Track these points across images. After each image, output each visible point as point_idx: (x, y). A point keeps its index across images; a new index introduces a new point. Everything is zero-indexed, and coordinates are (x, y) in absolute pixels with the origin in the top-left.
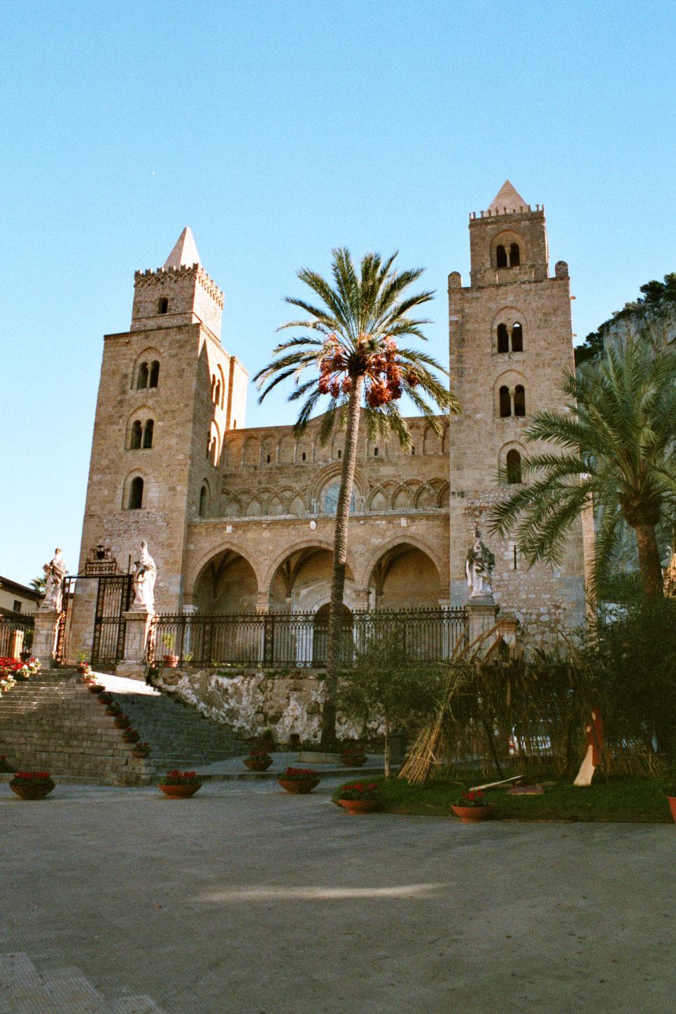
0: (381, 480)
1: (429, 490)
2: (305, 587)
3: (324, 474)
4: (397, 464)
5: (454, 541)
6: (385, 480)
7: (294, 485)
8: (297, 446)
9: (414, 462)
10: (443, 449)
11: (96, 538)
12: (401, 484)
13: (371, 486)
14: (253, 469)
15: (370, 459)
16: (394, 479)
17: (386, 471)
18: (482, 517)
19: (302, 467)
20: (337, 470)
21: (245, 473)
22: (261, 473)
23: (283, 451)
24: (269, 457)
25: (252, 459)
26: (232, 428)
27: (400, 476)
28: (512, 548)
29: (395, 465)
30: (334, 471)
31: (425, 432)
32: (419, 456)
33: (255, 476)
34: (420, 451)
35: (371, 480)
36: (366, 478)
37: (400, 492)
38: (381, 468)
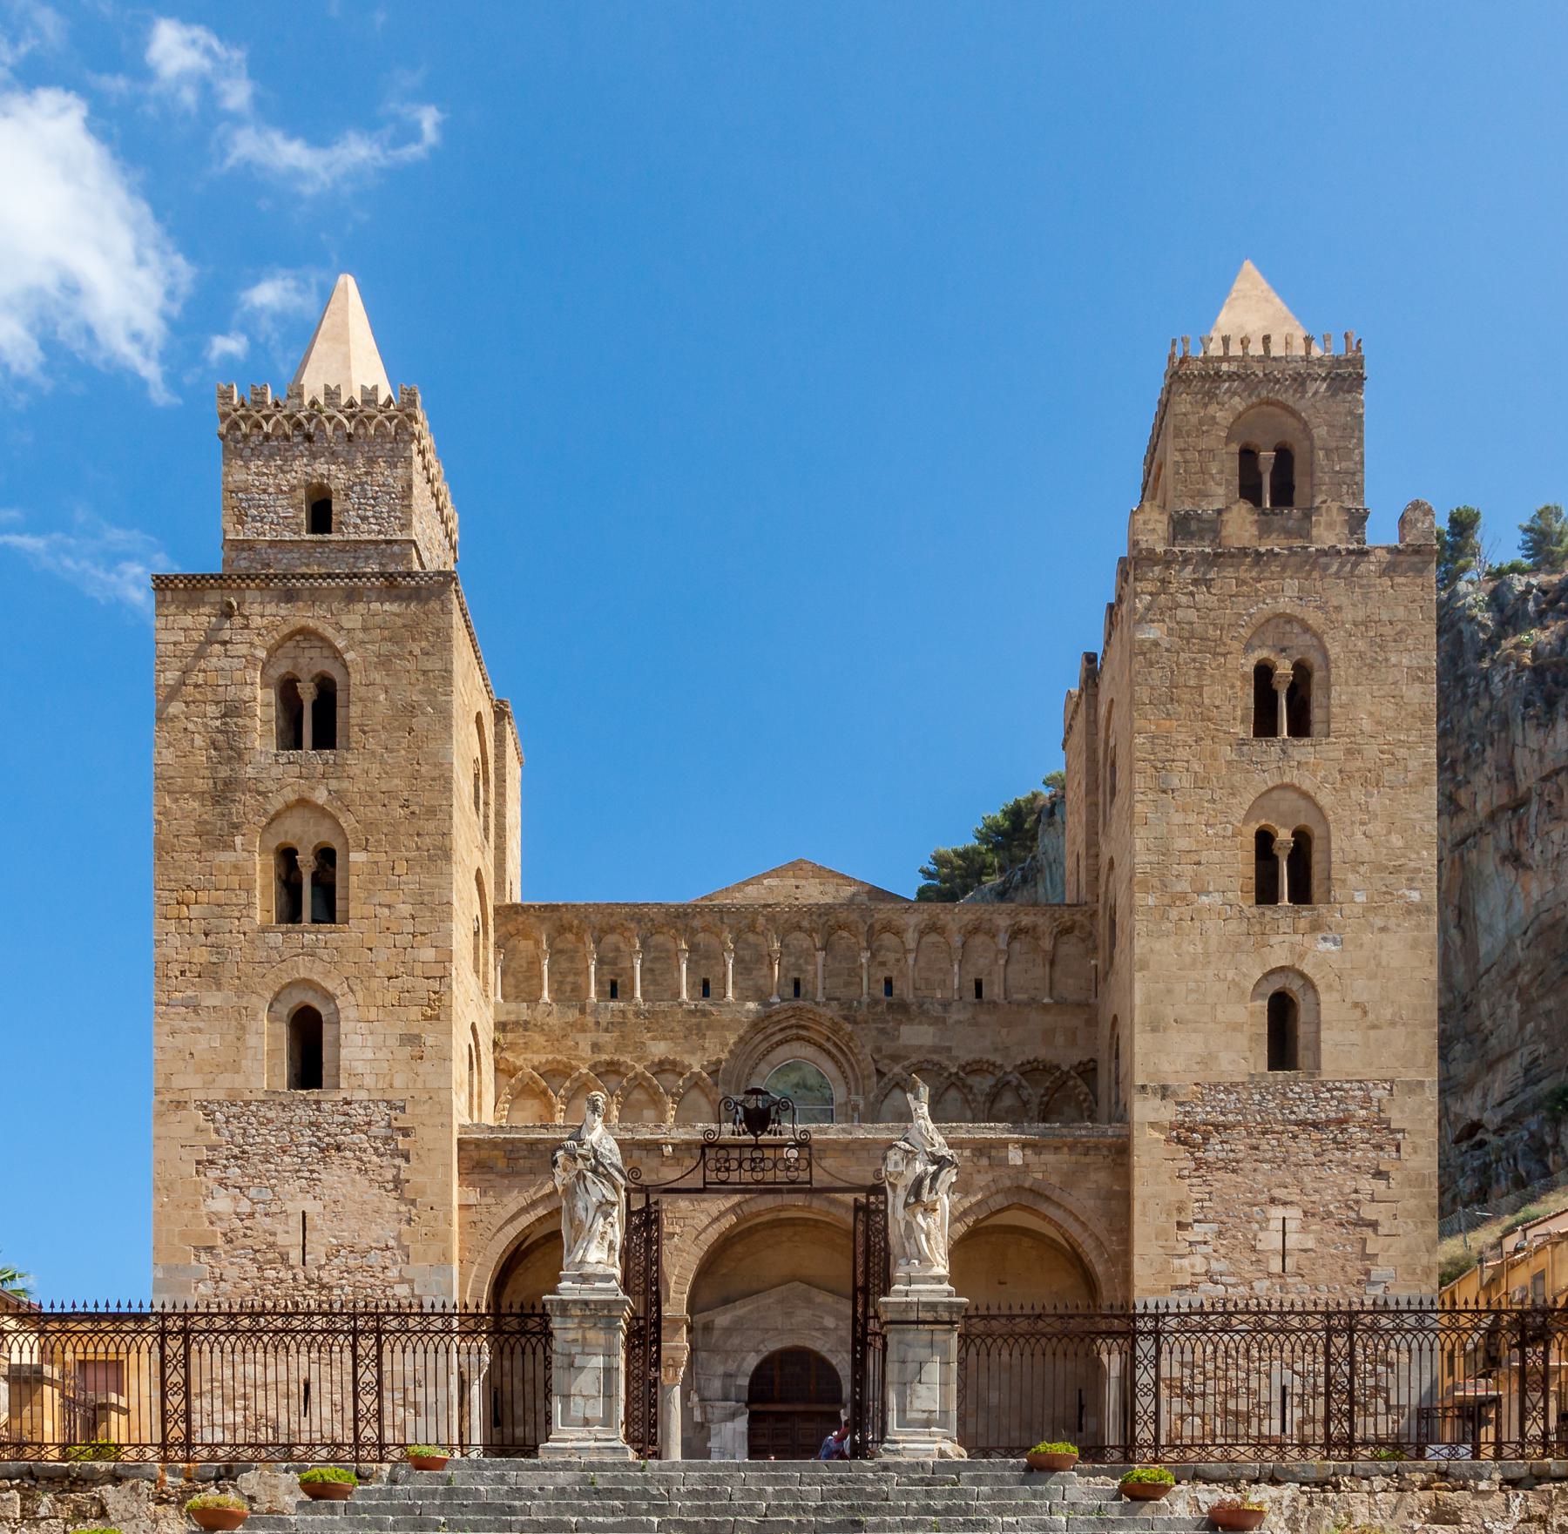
0: (906, 1058)
1: (1019, 1086)
2: (724, 1314)
3: (760, 1037)
4: (944, 1021)
5: (1144, 1204)
6: (914, 1060)
7: (687, 1059)
8: (689, 960)
9: (983, 1018)
10: (1051, 989)
11: (198, 1163)
12: (954, 1070)
13: (880, 1073)
14: (577, 1013)
15: (875, 1002)
16: (935, 1058)
17: (917, 1036)
18: (1208, 1147)
19: (705, 1013)
20: (791, 1027)
21: (552, 1020)
22: (598, 1023)
23: (652, 970)
24: (614, 985)
25: (568, 988)
26: (508, 901)
27: (949, 1049)
28: (1278, 1225)
29: (939, 1021)
30: (781, 1030)
31: (1008, 944)
32: (995, 1004)
33: (583, 1030)
34: (993, 991)
35: (876, 1057)
36: (868, 1050)
37: (947, 1089)
38: (905, 1030)
